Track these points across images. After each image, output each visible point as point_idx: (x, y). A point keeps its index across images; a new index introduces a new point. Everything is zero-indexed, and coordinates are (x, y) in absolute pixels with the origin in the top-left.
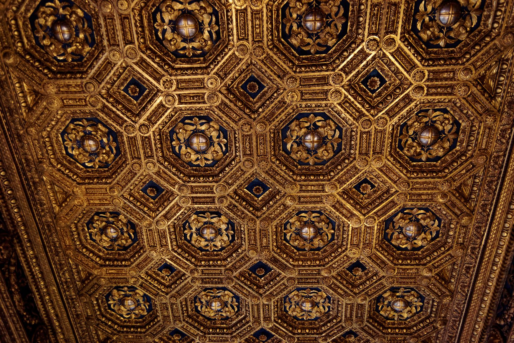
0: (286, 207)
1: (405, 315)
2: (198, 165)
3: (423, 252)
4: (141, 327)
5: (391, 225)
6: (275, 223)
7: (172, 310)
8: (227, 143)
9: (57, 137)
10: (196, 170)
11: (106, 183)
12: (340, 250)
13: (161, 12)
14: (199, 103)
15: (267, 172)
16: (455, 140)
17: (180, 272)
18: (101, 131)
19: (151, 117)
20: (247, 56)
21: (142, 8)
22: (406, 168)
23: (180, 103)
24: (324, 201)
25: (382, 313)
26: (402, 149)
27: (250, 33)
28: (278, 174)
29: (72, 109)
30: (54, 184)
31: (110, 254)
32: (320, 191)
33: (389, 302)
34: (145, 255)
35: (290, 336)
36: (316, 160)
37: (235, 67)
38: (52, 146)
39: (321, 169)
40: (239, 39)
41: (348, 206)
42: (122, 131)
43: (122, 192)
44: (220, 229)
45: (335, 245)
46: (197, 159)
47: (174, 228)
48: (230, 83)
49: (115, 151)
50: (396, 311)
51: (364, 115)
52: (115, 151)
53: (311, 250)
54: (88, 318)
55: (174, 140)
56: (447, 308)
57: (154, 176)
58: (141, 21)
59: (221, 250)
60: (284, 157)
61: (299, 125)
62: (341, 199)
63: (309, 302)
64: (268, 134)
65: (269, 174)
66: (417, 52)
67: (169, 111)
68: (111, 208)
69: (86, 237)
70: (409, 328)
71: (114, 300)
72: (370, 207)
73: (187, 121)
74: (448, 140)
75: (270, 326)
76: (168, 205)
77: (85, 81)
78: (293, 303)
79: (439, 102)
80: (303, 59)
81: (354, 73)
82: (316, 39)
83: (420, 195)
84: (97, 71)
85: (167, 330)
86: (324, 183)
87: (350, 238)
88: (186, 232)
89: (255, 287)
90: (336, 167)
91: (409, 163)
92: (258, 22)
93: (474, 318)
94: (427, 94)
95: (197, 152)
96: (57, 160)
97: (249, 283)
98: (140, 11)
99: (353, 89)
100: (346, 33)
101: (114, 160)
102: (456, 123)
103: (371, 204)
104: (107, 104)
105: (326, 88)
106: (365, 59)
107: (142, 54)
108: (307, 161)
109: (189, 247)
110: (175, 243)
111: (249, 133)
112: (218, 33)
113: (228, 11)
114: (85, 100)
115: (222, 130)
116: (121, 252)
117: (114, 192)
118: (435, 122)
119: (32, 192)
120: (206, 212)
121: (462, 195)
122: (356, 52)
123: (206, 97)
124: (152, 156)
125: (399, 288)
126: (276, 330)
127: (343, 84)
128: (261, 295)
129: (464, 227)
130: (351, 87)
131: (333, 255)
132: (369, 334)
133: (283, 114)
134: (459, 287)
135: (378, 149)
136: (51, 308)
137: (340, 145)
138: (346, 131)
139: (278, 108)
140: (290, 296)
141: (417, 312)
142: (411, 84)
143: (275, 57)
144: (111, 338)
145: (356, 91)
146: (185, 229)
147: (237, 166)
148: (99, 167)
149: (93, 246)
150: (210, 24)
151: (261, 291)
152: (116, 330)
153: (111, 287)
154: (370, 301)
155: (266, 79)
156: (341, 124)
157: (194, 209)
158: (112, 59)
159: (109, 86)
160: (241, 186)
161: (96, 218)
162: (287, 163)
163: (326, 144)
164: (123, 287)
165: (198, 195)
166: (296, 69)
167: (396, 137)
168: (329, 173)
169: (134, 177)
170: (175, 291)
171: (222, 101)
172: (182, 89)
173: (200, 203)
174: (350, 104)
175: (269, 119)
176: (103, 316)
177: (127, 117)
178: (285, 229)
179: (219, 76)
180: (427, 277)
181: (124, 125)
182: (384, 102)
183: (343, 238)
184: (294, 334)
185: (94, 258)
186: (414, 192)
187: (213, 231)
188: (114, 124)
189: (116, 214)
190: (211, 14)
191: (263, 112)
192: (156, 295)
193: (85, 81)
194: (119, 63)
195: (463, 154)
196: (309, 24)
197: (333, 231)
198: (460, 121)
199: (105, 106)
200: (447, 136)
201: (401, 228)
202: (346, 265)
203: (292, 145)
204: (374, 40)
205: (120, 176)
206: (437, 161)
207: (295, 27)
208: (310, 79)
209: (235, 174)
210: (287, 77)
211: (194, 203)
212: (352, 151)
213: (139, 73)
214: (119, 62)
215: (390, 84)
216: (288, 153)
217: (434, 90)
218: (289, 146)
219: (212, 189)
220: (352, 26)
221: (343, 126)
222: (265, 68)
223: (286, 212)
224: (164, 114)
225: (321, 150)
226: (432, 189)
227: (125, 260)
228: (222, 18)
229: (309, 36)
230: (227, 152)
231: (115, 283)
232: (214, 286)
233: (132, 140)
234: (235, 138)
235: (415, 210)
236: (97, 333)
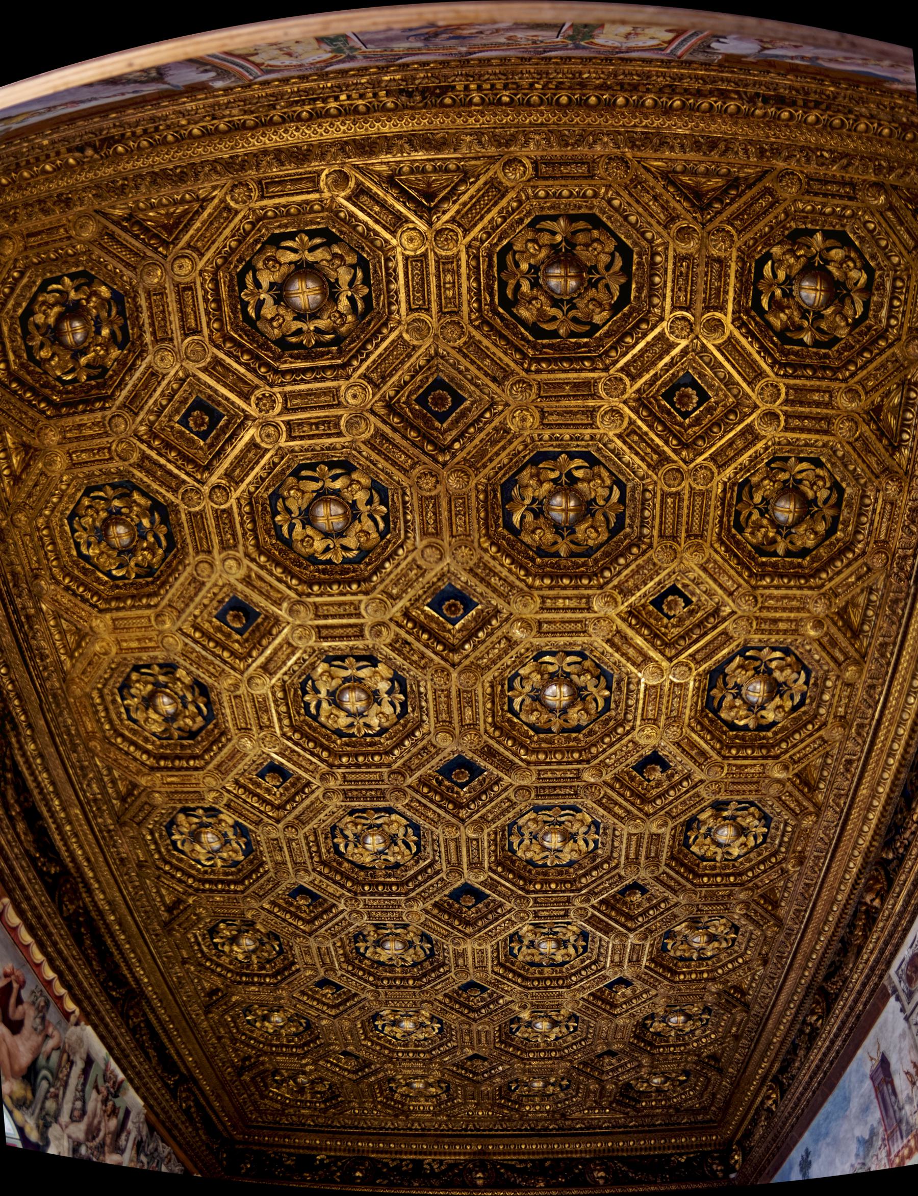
1: (736, 852)
2: (329, 562)
3: (775, 733)
4: (236, 883)
5: (721, 681)
6: (489, 676)
7: (290, 852)
8: (387, 515)
10: (324, 572)
12: (620, 730)
13: (255, 271)
14: (329, 436)
15: (471, 570)
16: (835, 519)
17: (299, 778)
18: (139, 505)
19: (233, 471)
20: (429, 341)
21: (218, 267)
22: (748, 569)
23: (291, 438)
24: (591, 630)
25: (694, 849)
26: (741, 530)
27: (434, 297)
28: (495, 574)
29: (86, 470)
30: (60, 616)
31: (165, 747)
32: (581, 610)
33: (709, 829)
34: (230, 746)
35: (520, 897)
36: (573, 547)
37: (402, 362)
38: (53, 543)
39: (584, 564)
40: (410, 310)
41: (639, 641)
42: (177, 501)
44: (376, 692)
45: (611, 720)
46: (327, 549)
47: (284, 691)
48: (392, 393)
49: (164, 543)
50: (719, 845)
51: (668, 460)
52: (164, 543)
53: (563, 730)
54: (140, 865)
56: (806, 835)
57: (240, 587)
58: (216, 290)
59: (379, 734)
60: (509, 540)
61: (538, 475)
62: (624, 627)
63: (559, 832)
64: (473, 494)
65: (476, 575)
66: (763, 349)
67: (268, 456)
68: (160, 655)
69: (119, 714)
70: (740, 874)
71: (181, 833)
72: (682, 642)
73: (304, 473)
74: (824, 518)
75: (482, 878)
77: (108, 414)
78: (527, 836)
79: (806, 445)
80: (544, 346)
81: (647, 377)
82: (569, 310)
84: (130, 392)
85: (283, 887)
86: (590, 592)
87: (640, 705)
88: (307, 698)
89: (451, 806)
90: (615, 560)
92: (449, 278)
93: (849, 851)
94: (786, 429)
96: (63, 568)
97: (438, 798)
98: (215, 274)
99: (645, 407)
100: (629, 302)
101: (163, 560)
102: (836, 487)
103: (682, 637)
104: (148, 451)
105: (591, 403)
106: (667, 352)
107: (215, 350)
108: (554, 549)
109: (315, 730)
110: (286, 722)
112: (367, 299)
113: (387, 260)
114: (109, 449)
115: (378, 490)
116: (185, 742)
117: (164, 622)
119: (26, 634)
120: (347, 656)
121: (848, 624)
122: (649, 338)
123: (342, 423)
125: (727, 803)
126: (493, 885)
127: (625, 396)
128: (463, 821)
129: (848, 685)
130: (641, 403)
131: (607, 740)
132: (669, 887)
133: (503, 454)
134: (832, 797)
135: (696, 529)
136: (78, 848)
137: (621, 517)
138: (634, 489)
139: (494, 443)
140: (521, 822)
141: (757, 846)
142: (756, 407)
143: (486, 342)
144: (184, 902)
145: (651, 413)
146: (305, 693)
147: (409, 559)
148: (138, 576)
149: (134, 732)
150: (351, 284)
151: (463, 813)
152: (190, 886)
153: (174, 808)
154: (675, 828)
155: (468, 385)
157: (322, 651)
158: (160, 366)
159: (152, 418)
160: (417, 600)
161: (134, 676)
163: (593, 516)
164: (194, 809)
165: (330, 622)
166: (530, 365)
167: (730, 505)
168: (602, 572)
170: (293, 815)
171: (377, 430)
172: (295, 410)
173: (333, 638)
174: (640, 437)
175: (474, 464)
176: (167, 862)
177: (187, 474)
178: (511, 688)
179: (370, 381)
180: (779, 781)
181: (181, 491)
182: (706, 435)
183: (627, 706)
184: (528, 892)
185: (138, 754)
187: (363, 696)
188: (162, 491)
189: (169, 668)
190: (353, 266)
191: (462, 449)
192: (258, 823)
193: (108, 414)
194: (173, 372)
196: (553, 282)
197: (607, 693)
198: (844, 485)
199: (145, 457)
200: (821, 509)
201: (738, 686)
202: (632, 760)
203: (523, 517)
204: (684, 318)
205: (173, 591)
206: (804, 558)
207: (525, 287)
208: (560, 385)
209: (406, 575)
210: (512, 380)
211: (321, 638)
212: (646, 531)
213: (210, 387)
214: (172, 369)
215: (717, 403)
216: (516, 532)
217: (797, 422)
218: (516, 518)
219: (357, 608)
220: (639, 290)
222: (464, 363)
223: (513, 653)
224: (257, 463)
225: (583, 527)
226: (798, 610)
227: (195, 757)
228: (375, 272)
229: (556, 303)
231: (180, 801)
232: (368, 804)
233: (197, 519)
234: (405, 503)
235: (766, 650)
236: (158, 892)
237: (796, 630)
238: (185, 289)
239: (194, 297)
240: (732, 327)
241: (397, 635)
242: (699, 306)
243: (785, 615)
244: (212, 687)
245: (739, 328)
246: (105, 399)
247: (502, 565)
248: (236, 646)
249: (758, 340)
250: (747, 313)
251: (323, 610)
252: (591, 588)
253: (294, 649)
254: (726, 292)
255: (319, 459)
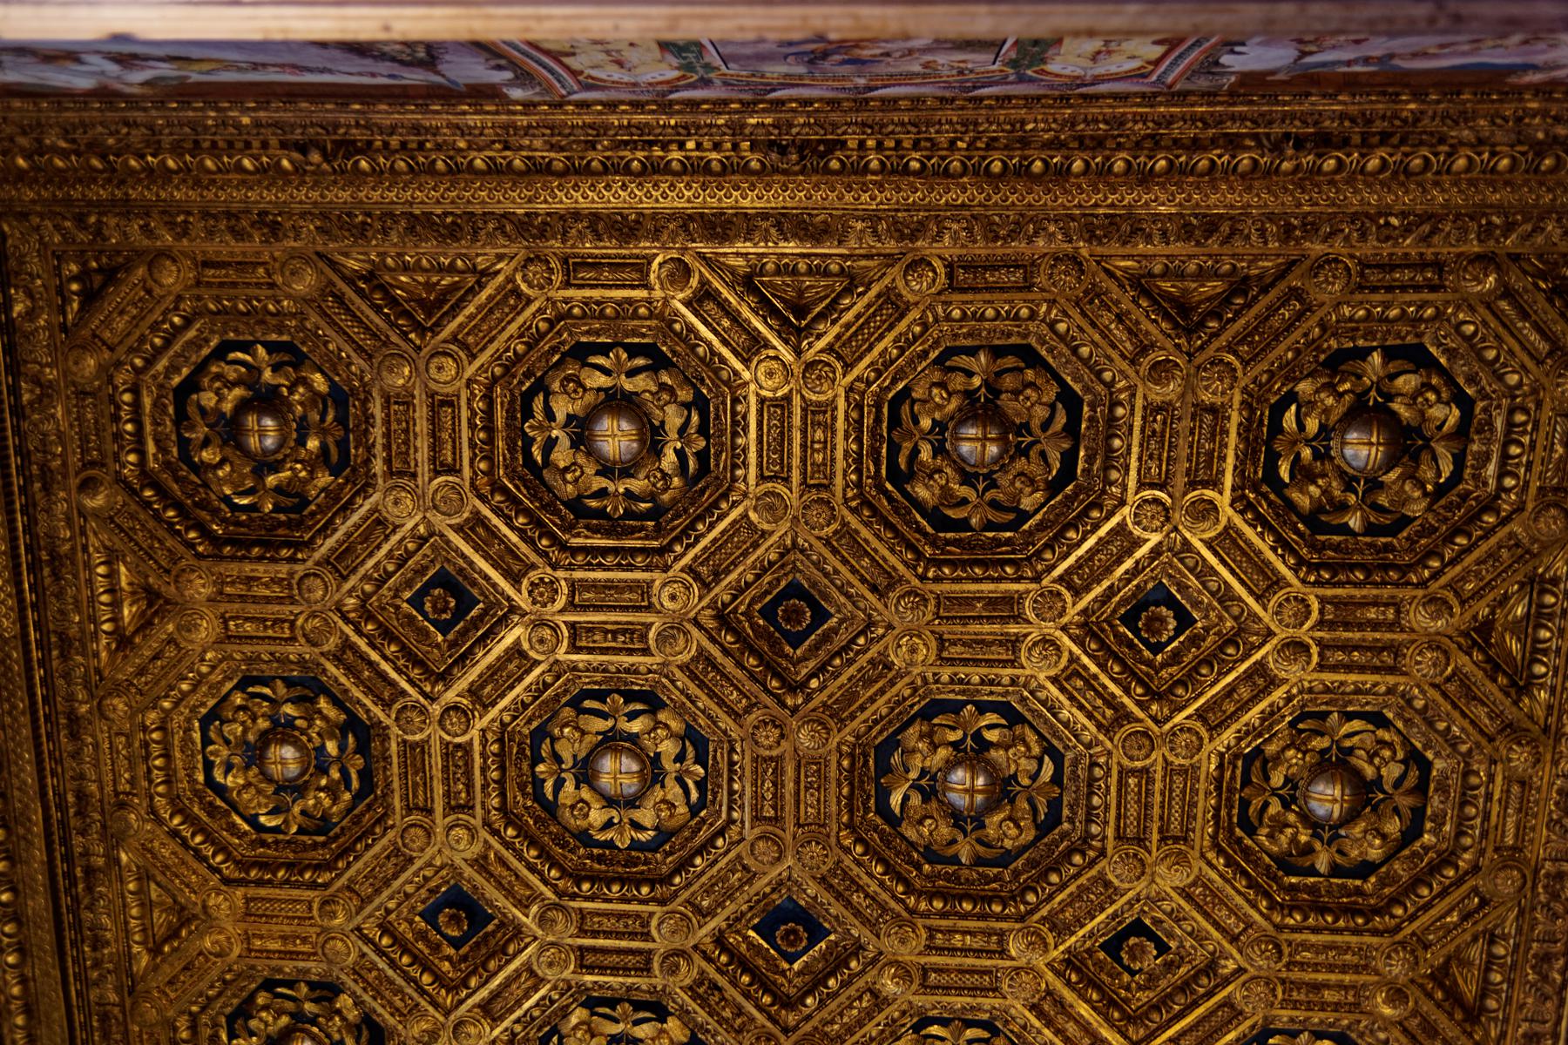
0: (880, 1001)
2: (610, 844)
8: (705, 779)
9: (188, 730)
10: (600, 859)
11: (313, 885)
13: (548, 394)
14: (630, 652)
15: (823, 879)
16: (1418, 814)
18: (325, 718)
19: (482, 687)
20: (784, 526)
21: (495, 380)
23: (574, 648)
24: (1005, 987)
26: (1251, 831)
27: (796, 462)
28: (860, 888)
29: (247, 649)
30: (150, 877)
32: (990, 953)
36: (979, 848)
37: (745, 554)
38: (167, 756)
39: (996, 878)
40: (762, 478)
41: (1084, 1010)
42: (387, 721)
43: (360, 918)
46: (608, 825)
48: (727, 598)
49: (355, 784)
51: (1130, 718)
52: (355, 784)
55: (542, 761)
57: (468, 872)
58: (489, 413)
60: (881, 833)
61: (930, 735)
62: (1058, 985)
64: (834, 759)
66: (1281, 543)
67: (537, 671)
68: (315, 968)
73: (588, 704)
74: (1396, 811)
76: (500, 968)
77: (300, 569)
79: (1358, 691)
80: (948, 542)
81: (1098, 590)
82: (986, 490)
83: (1317, 987)
84: (340, 543)
86: (1004, 925)
90: (1044, 876)
91: (1275, 878)
92: (819, 435)
94: (1321, 667)
95: (610, 802)
98: (490, 388)
99: (1095, 636)
100: (1074, 477)
101: (349, 811)
102: (1415, 759)
103: (1156, 1008)
104: (355, 638)
105: (1013, 629)
106: (1130, 553)
107: (478, 503)
108: (951, 851)
111: (774, 753)
112: (702, 456)
113: (735, 401)
114: (292, 624)
115: (693, 739)
117: (334, 915)
118: (1351, 750)
119: (76, 900)
120: (619, 1001)
121: (1454, 996)
122: (1102, 532)
123: (652, 634)
124: (468, 807)
127: (1065, 620)
130: (1088, 630)
133: (881, 701)
135: (1175, 828)
137: (1055, 805)
138: (1075, 762)
139: (869, 682)
142: (1270, 634)
143: (865, 533)
145: (1103, 645)
147: (732, 855)
150: (682, 431)
155: (835, 594)
156: (1060, 739)
158: (391, 512)
159: (368, 588)
160: (738, 920)
162: (889, 854)
163: (1012, 801)
166: (926, 570)
167: (1231, 790)
169: (403, 869)
171: (701, 650)
172: (584, 608)
173: (603, 969)
174: (1086, 682)
175: (836, 713)
177: (410, 681)
179: (697, 577)
181: (397, 706)
182: (1190, 679)
186: (1296, 975)
188: (367, 702)
189: (327, 991)
190: (687, 406)
191: (821, 689)
193: (300, 569)
194: (410, 525)
195: (1447, 858)
196: (965, 448)
198: (1430, 755)
199: (347, 645)
200: (1390, 797)
203: (906, 798)
204: (1156, 501)
206: (1365, 878)
207: (925, 454)
208: (968, 601)
209: (724, 879)
210: (899, 591)
211: (583, 967)
212: (1095, 829)
213: (463, 556)
214: (409, 519)
215: (1206, 629)
216: (893, 821)
217: (1340, 656)
218: (896, 799)
219: (646, 924)
220: (1090, 459)
221: (1067, 747)
222: (833, 562)
223: (880, 1017)
224: (520, 679)
225: (997, 818)
226: (1356, 969)
228: (717, 417)
229: (967, 479)
230: (704, 807)
233: (415, 753)
234: (732, 764)
237: (1357, 1005)
238: (443, 403)
239: (456, 418)
240: (1230, 511)
241: (702, 972)
242: (1180, 481)
243: (1333, 977)
244: (393, 1032)
245: (1242, 512)
246: (298, 546)
247: (871, 875)
248: (446, 966)
249: (1272, 530)
250: (1255, 488)
251: (592, 923)
252: (1005, 918)
253: (540, 982)
254: (1223, 458)
255: (612, 685)
